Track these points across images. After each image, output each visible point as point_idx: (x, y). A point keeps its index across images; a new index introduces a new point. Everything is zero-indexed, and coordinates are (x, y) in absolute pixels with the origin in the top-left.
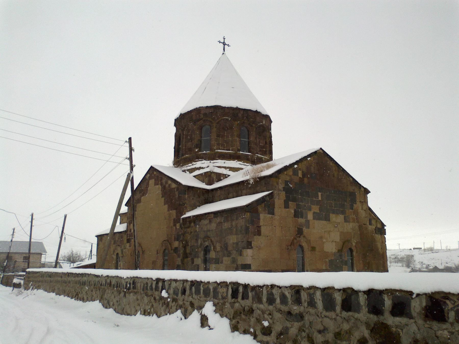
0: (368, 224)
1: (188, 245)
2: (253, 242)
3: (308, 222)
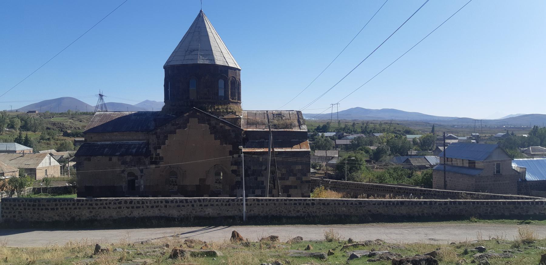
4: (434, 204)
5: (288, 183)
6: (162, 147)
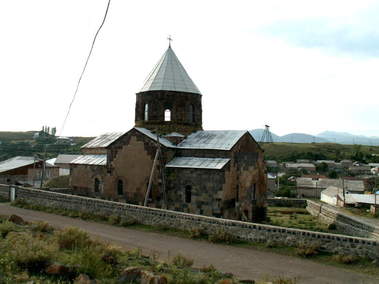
3: (241, 172)
5: (201, 199)
6: (114, 159)
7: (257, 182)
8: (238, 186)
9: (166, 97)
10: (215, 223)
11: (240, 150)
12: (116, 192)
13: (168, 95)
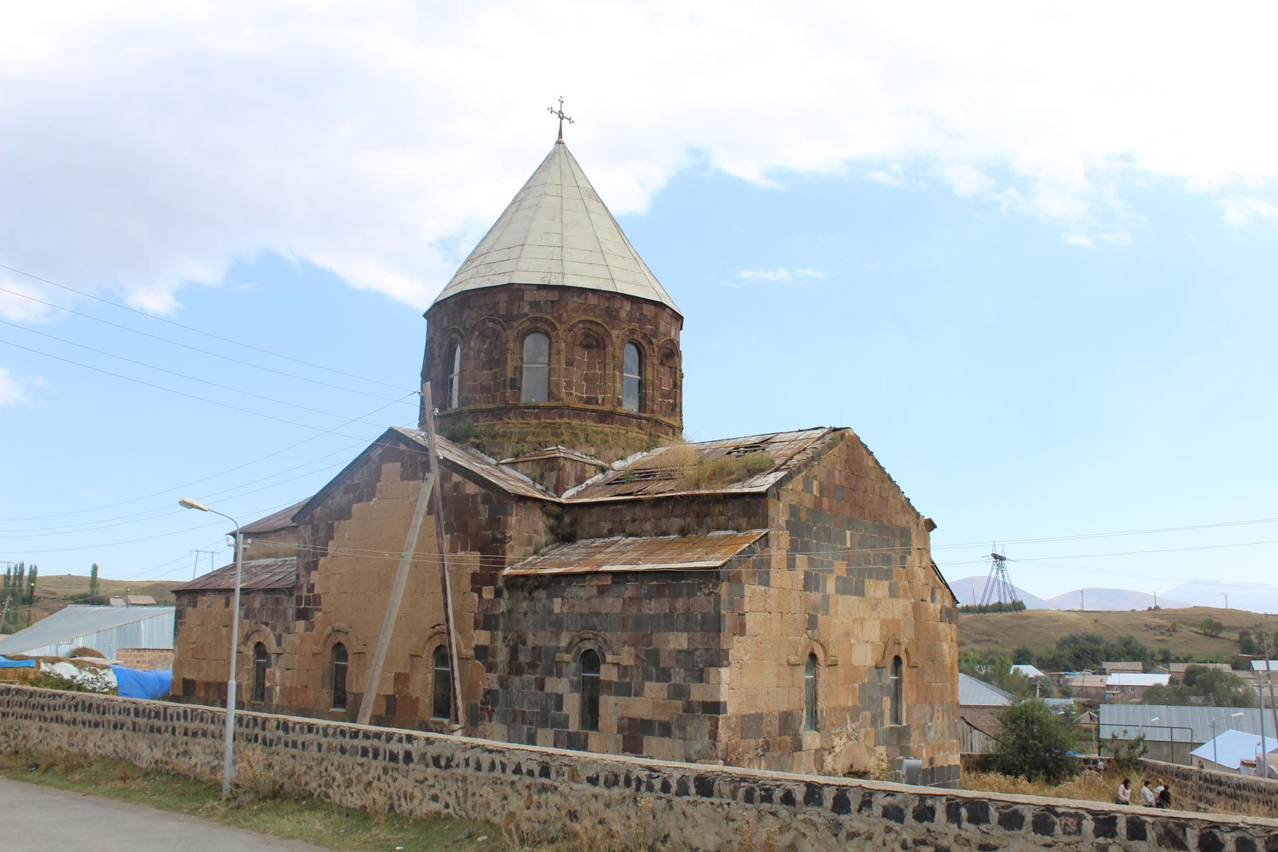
0: (929, 599)
1: (524, 643)
2: (731, 652)
3: (826, 598)
4: (860, 810)
5: (640, 708)
7: (906, 650)
8: (813, 656)
9: (526, 309)
10: (616, 783)
11: (818, 502)
12: (326, 696)
13: (535, 304)
